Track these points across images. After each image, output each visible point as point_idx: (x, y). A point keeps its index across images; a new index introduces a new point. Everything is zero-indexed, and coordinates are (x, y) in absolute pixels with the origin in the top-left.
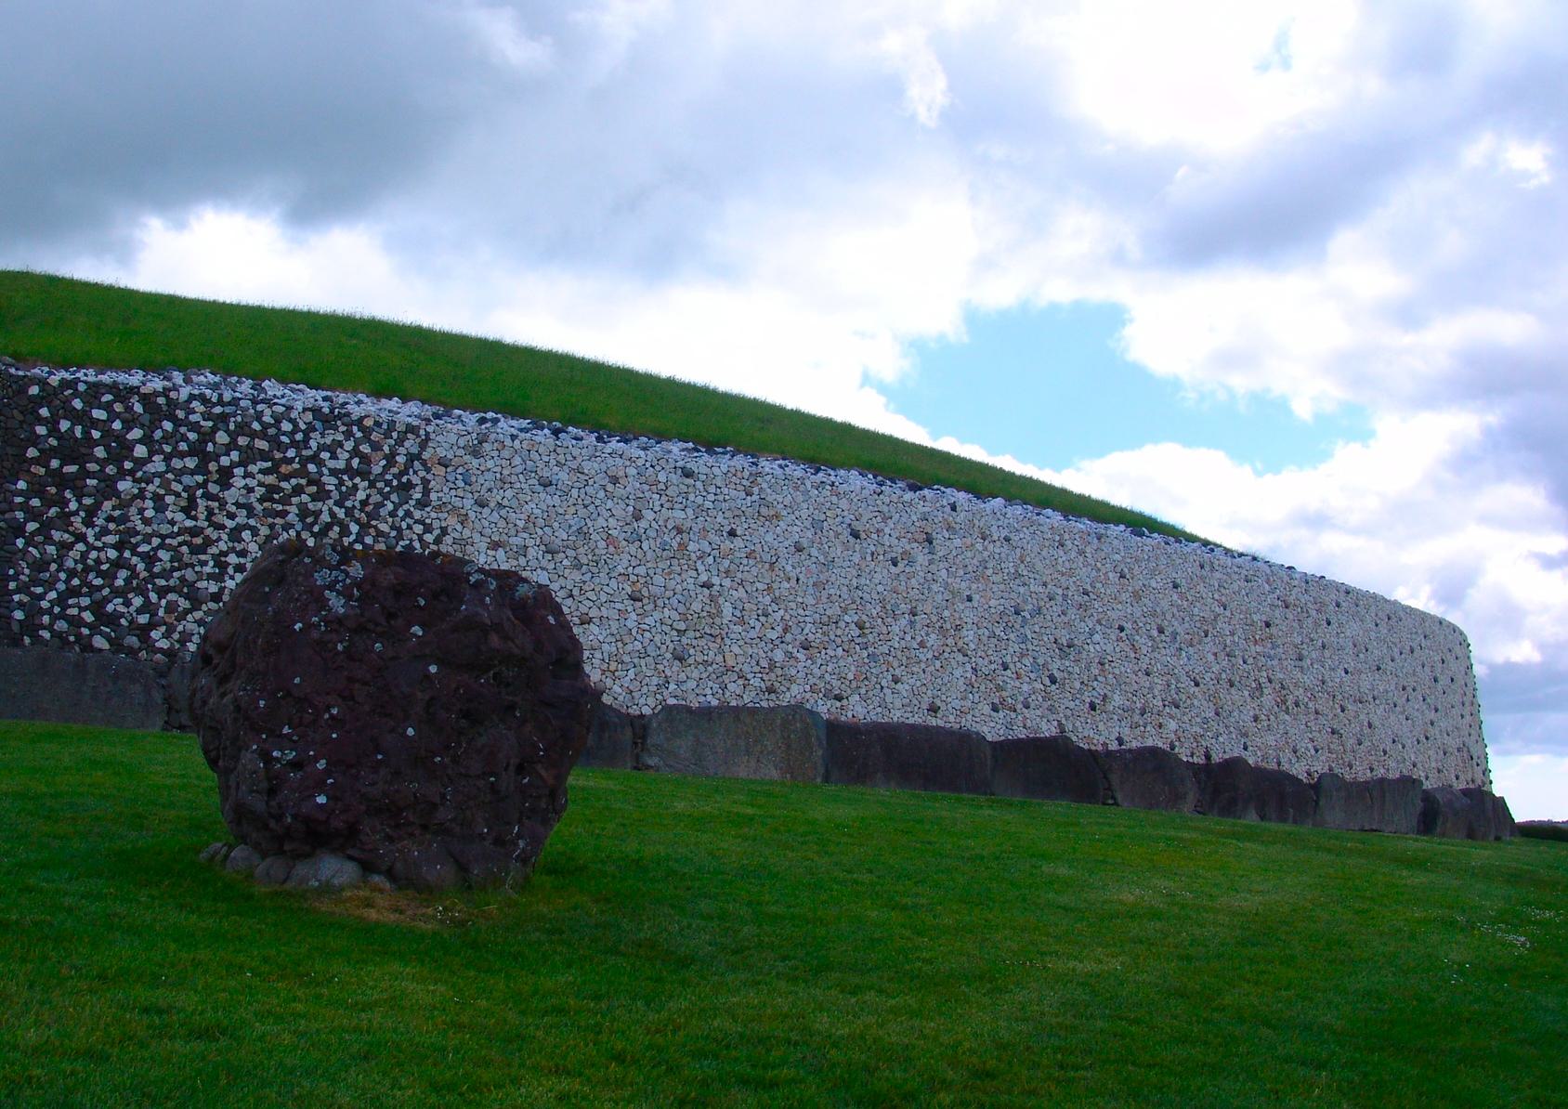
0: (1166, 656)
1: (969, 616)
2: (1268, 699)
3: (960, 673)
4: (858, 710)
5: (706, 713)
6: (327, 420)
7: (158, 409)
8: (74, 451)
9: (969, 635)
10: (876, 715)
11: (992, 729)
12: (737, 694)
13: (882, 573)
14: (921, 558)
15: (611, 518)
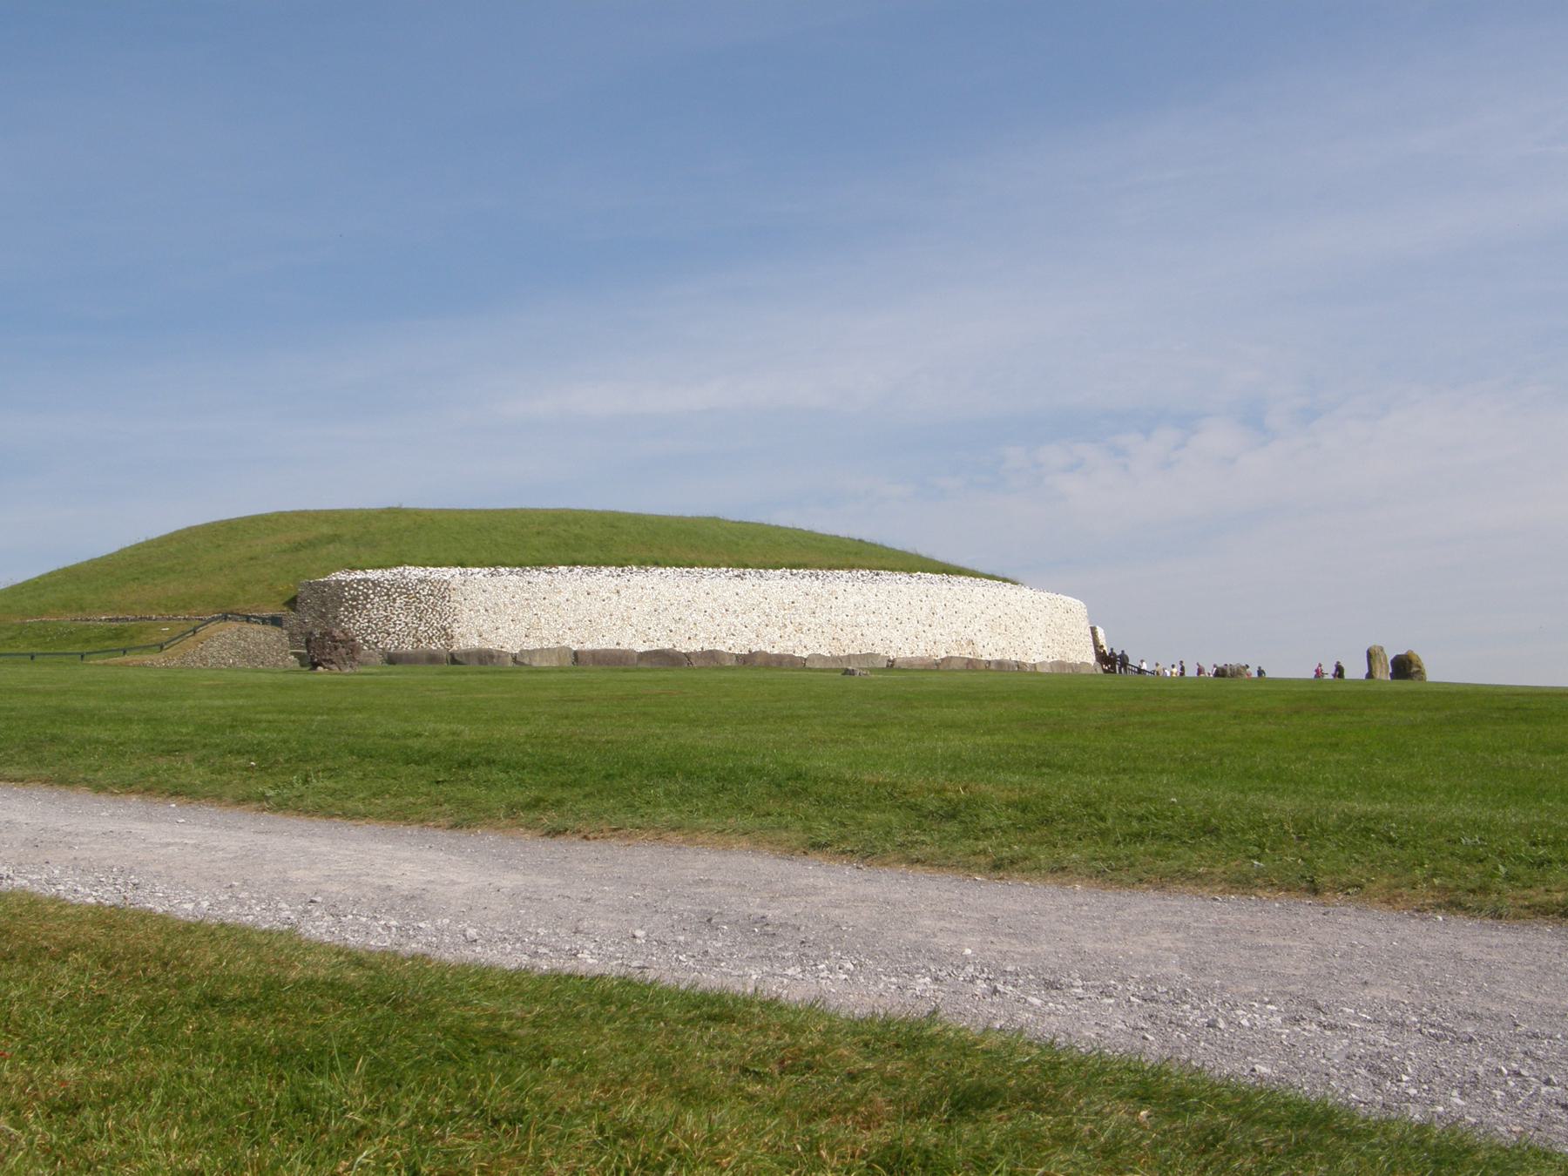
0: (731, 618)
1: (634, 613)
2: (790, 628)
3: (630, 631)
4: (589, 646)
5: (534, 651)
6: (421, 581)
7: (376, 584)
8: (355, 599)
9: (634, 621)
10: (596, 647)
11: (641, 647)
12: (545, 644)
13: (599, 605)
14: (615, 597)
15: (506, 598)
